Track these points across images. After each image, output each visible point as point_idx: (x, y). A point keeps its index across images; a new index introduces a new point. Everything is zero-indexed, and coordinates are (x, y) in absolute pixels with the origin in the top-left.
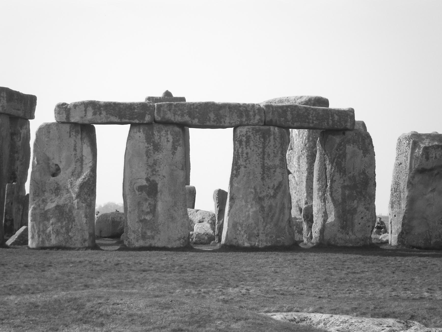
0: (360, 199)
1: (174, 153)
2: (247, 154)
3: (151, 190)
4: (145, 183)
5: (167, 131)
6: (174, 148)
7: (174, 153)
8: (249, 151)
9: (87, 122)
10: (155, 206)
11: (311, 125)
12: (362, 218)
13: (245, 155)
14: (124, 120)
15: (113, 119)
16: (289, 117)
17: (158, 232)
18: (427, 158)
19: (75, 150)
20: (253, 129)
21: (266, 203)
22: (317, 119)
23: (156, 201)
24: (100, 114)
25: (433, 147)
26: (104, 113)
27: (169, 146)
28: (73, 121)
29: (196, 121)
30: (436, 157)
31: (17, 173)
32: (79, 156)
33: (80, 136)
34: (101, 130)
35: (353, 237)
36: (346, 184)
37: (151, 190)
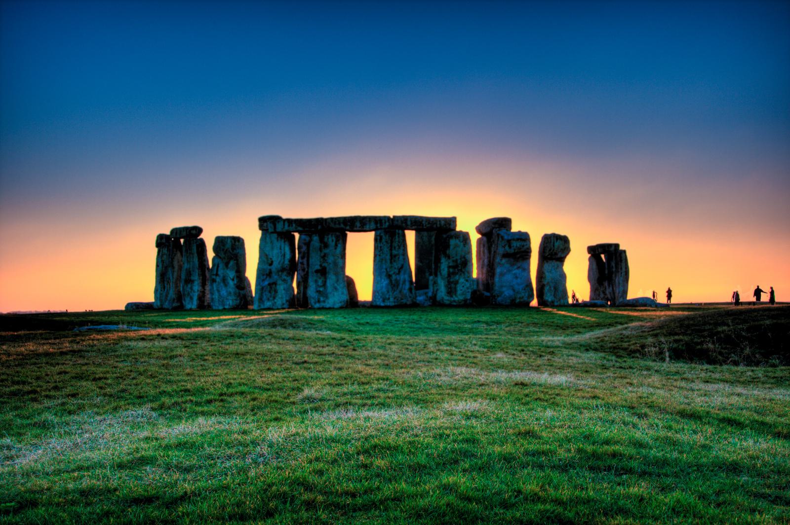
0: (461, 274)
1: (336, 249)
5: (332, 235)
6: (336, 245)
8: (382, 245)
12: (463, 286)
13: (379, 248)
16: (409, 223)
17: (327, 297)
18: (510, 247)
19: (281, 249)
21: (394, 277)
22: (429, 223)
23: (326, 278)
24: (292, 226)
26: (294, 225)
30: (516, 247)
32: (283, 253)
33: (283, 240)
35: (456, 299)
36: (451, 264)
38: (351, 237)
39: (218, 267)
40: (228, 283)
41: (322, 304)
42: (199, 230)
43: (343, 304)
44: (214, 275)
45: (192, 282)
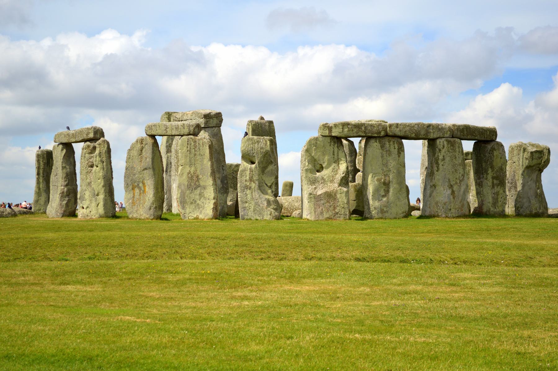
1: (399, 156)
5: (394, 142)
7: (399, 156)
16: (465, 132)
19: (334, 154)
23: (389, 188)
27: (396, 151)
28: (333, 134)
33: (336, 145)
35: (498, 210)
45: (205, 188)
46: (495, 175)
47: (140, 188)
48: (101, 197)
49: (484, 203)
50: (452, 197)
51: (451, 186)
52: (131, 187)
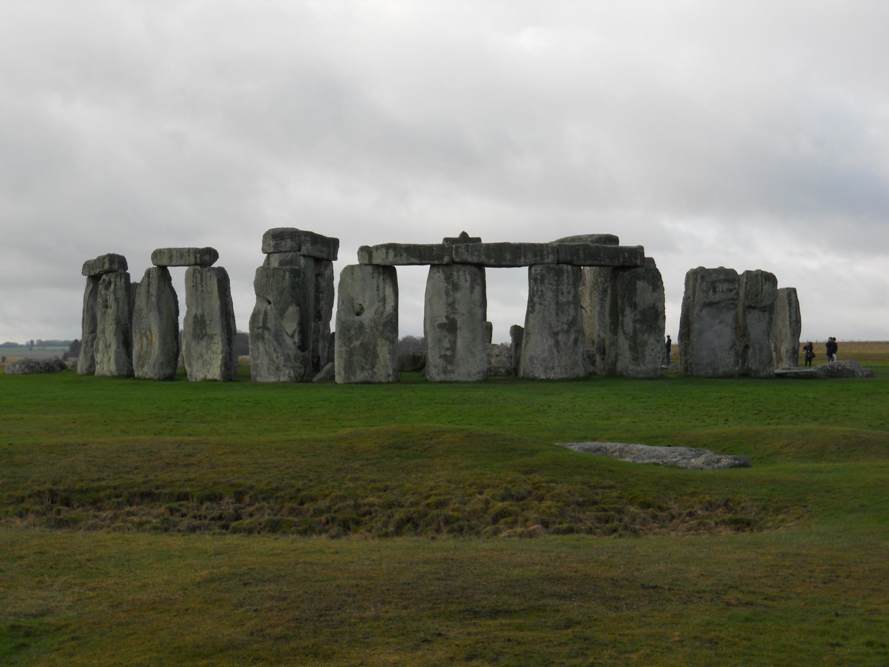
1: (472, 292)
2: (542, 291)
3: (450, 327)
4: (444, 320)
6: (472, 288)
7: (472, 292)
9: (388, 264)
10: (455, 343)
11: (603, 263)
13: (540, 293)
14: (424, 262)
15: (413, 260)
16: (581, 255)
18: (715, 292)
19: (378, 290)
20: (547, 268)
21: (561, 337)
23: (456, 337)
24: (401, 255)
25: (719, 281)
26: (405, 255)
27: (467, 285)
28: (374, 262)
29: (492, 261)
31: (323, 313)
32: (381, 295)
33: (381, 277)
34: (402, 271)
35: (644, 368)
37: (450, 327)
38: (491, 273)
39: (266, 313)
40: (284, 341)
41: (449, 377)
42: (211, 254)
43: (481, 374)
44: (258, 328)
45: (211, 337)
46: (638, 317)
47: (147, 337)
48: (114, 347)
49: (620, 357)
50: (555, 350)
51: (556, 334)
52: (138, 335)
